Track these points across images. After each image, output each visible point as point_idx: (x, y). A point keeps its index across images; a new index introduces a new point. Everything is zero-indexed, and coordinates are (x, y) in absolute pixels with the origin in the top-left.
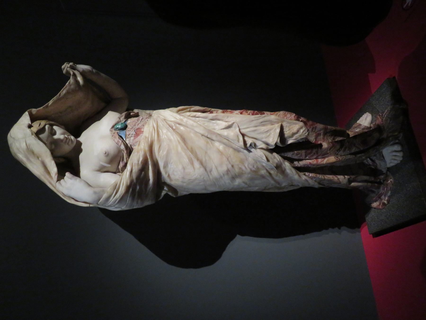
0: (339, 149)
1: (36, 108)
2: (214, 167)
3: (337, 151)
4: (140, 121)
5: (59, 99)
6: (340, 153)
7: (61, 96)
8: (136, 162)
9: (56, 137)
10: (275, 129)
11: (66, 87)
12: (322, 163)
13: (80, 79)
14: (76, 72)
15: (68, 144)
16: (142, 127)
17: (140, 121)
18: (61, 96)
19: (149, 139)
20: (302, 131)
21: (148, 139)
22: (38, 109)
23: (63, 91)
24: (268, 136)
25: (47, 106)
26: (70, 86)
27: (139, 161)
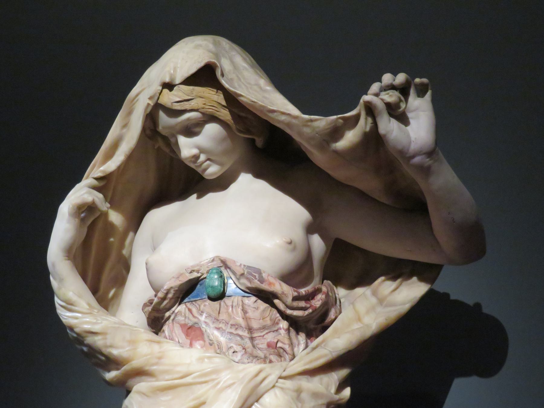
4: (233, 331)
8: (109, 342)
16: (207, 341)
17: (233, 331)
19: (155, 368)
21: (156, 364)
26: (308, 126)
27: (111, 346)
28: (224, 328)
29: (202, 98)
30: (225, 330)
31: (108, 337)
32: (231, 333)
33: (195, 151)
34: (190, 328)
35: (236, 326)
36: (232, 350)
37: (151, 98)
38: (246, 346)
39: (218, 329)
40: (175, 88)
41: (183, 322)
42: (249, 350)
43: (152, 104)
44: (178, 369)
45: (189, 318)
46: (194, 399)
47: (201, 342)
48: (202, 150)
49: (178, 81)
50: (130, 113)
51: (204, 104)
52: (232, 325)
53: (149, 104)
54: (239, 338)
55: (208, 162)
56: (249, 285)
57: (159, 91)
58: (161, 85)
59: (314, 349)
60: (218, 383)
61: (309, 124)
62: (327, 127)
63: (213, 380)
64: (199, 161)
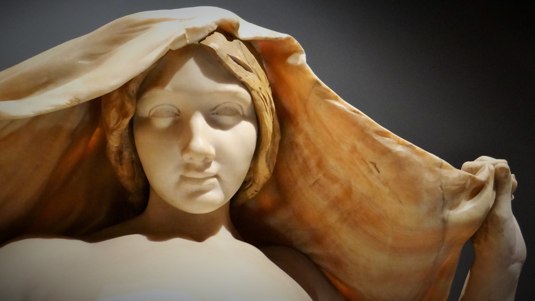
1: (308, 62)
5: (363, 133)
7: (378, 138)
9: (199, 122)
11: (418, 153)
13: (467, 209)
14: (488, 194)
15: (183, 179)
18: (378, 138)
22: (308, 68)
23: (398, 145)
25: (324, 96)
26: (431, 170)
29: (260, 79)
33: (212, 151)
40: (234, 40)
43: (188, 42)
48: (221, 156)
50: (117, 41)
51: (260, 88)
55: (215, 180)
57: (212, 30)
58: (216, 23)
61: (437, 169)
62: (456, 182)
64: (207, 170)
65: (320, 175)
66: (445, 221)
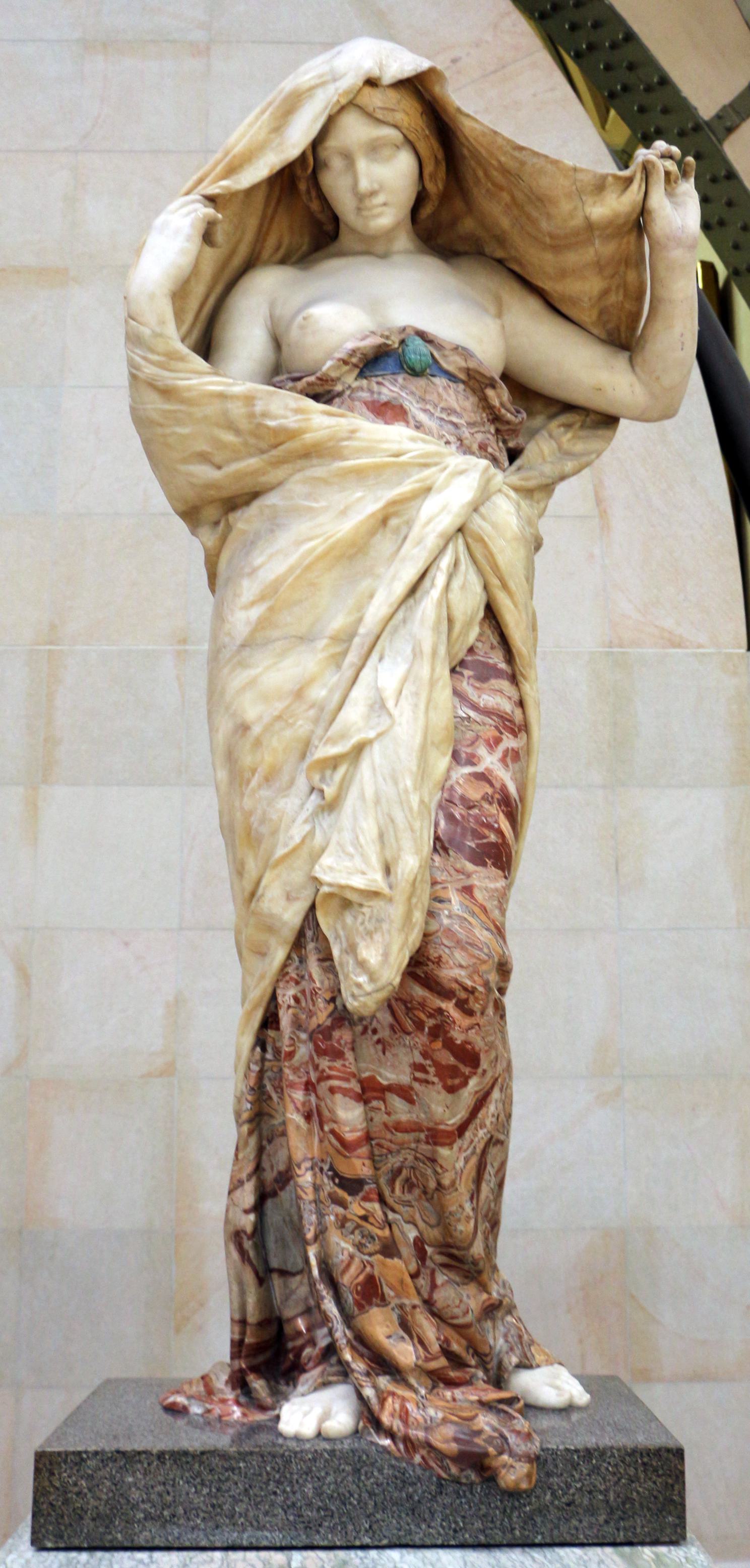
0: (341, 1178)
2: (252, 672)
3: (331, 1168)
4: (444, 416)
6: (326, 1180)
10: (363, 873)
12: (291, 1107)
16: (412, 422)
17: (444, 416)
20: (362, 979)
21: (349, 438)
24: (344, 851)
28: (432, 411)
30: (433, 414)
31: (256, 402)
32: (442, 419)
34: (386, 404)
35: (450, 411)
36: (445, 440)
37: (346, 93)
38: (464, 436)
39: (425, 411)
41: (369, 399)
42: (466, 442)
44: (385, 446)
45: (380, 393)
46: (417, 482)
47: (403, 423)
49: (387, 79)
52: (443, 409)
53: (338, 101)
54: (451, 427)
56: (463, 364)
57: (358, 88)
59: (519, 469)
60: (445, 468)
63: (436, 464)
65: (489, 185)
66: (587, 218)
